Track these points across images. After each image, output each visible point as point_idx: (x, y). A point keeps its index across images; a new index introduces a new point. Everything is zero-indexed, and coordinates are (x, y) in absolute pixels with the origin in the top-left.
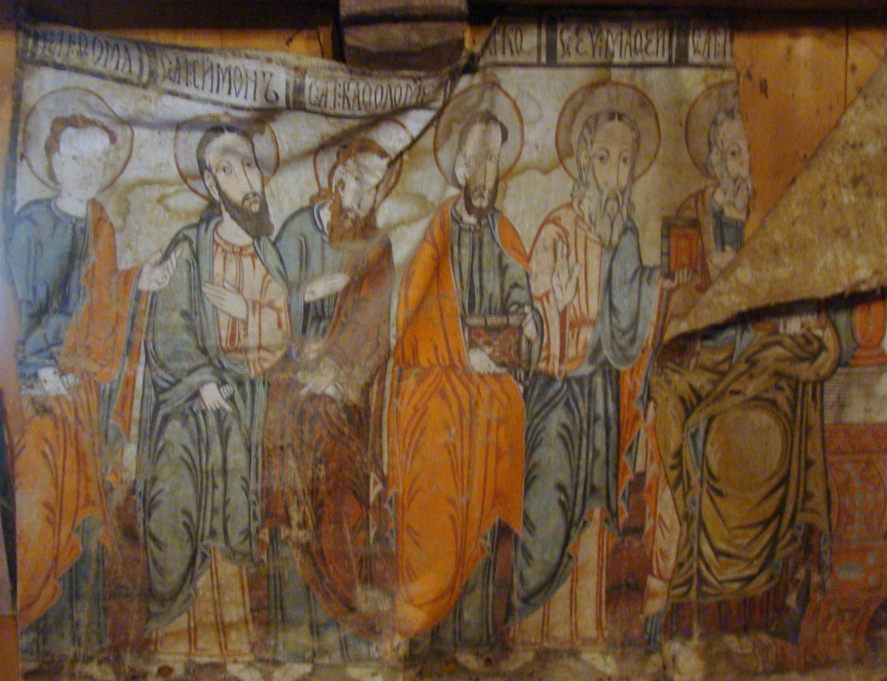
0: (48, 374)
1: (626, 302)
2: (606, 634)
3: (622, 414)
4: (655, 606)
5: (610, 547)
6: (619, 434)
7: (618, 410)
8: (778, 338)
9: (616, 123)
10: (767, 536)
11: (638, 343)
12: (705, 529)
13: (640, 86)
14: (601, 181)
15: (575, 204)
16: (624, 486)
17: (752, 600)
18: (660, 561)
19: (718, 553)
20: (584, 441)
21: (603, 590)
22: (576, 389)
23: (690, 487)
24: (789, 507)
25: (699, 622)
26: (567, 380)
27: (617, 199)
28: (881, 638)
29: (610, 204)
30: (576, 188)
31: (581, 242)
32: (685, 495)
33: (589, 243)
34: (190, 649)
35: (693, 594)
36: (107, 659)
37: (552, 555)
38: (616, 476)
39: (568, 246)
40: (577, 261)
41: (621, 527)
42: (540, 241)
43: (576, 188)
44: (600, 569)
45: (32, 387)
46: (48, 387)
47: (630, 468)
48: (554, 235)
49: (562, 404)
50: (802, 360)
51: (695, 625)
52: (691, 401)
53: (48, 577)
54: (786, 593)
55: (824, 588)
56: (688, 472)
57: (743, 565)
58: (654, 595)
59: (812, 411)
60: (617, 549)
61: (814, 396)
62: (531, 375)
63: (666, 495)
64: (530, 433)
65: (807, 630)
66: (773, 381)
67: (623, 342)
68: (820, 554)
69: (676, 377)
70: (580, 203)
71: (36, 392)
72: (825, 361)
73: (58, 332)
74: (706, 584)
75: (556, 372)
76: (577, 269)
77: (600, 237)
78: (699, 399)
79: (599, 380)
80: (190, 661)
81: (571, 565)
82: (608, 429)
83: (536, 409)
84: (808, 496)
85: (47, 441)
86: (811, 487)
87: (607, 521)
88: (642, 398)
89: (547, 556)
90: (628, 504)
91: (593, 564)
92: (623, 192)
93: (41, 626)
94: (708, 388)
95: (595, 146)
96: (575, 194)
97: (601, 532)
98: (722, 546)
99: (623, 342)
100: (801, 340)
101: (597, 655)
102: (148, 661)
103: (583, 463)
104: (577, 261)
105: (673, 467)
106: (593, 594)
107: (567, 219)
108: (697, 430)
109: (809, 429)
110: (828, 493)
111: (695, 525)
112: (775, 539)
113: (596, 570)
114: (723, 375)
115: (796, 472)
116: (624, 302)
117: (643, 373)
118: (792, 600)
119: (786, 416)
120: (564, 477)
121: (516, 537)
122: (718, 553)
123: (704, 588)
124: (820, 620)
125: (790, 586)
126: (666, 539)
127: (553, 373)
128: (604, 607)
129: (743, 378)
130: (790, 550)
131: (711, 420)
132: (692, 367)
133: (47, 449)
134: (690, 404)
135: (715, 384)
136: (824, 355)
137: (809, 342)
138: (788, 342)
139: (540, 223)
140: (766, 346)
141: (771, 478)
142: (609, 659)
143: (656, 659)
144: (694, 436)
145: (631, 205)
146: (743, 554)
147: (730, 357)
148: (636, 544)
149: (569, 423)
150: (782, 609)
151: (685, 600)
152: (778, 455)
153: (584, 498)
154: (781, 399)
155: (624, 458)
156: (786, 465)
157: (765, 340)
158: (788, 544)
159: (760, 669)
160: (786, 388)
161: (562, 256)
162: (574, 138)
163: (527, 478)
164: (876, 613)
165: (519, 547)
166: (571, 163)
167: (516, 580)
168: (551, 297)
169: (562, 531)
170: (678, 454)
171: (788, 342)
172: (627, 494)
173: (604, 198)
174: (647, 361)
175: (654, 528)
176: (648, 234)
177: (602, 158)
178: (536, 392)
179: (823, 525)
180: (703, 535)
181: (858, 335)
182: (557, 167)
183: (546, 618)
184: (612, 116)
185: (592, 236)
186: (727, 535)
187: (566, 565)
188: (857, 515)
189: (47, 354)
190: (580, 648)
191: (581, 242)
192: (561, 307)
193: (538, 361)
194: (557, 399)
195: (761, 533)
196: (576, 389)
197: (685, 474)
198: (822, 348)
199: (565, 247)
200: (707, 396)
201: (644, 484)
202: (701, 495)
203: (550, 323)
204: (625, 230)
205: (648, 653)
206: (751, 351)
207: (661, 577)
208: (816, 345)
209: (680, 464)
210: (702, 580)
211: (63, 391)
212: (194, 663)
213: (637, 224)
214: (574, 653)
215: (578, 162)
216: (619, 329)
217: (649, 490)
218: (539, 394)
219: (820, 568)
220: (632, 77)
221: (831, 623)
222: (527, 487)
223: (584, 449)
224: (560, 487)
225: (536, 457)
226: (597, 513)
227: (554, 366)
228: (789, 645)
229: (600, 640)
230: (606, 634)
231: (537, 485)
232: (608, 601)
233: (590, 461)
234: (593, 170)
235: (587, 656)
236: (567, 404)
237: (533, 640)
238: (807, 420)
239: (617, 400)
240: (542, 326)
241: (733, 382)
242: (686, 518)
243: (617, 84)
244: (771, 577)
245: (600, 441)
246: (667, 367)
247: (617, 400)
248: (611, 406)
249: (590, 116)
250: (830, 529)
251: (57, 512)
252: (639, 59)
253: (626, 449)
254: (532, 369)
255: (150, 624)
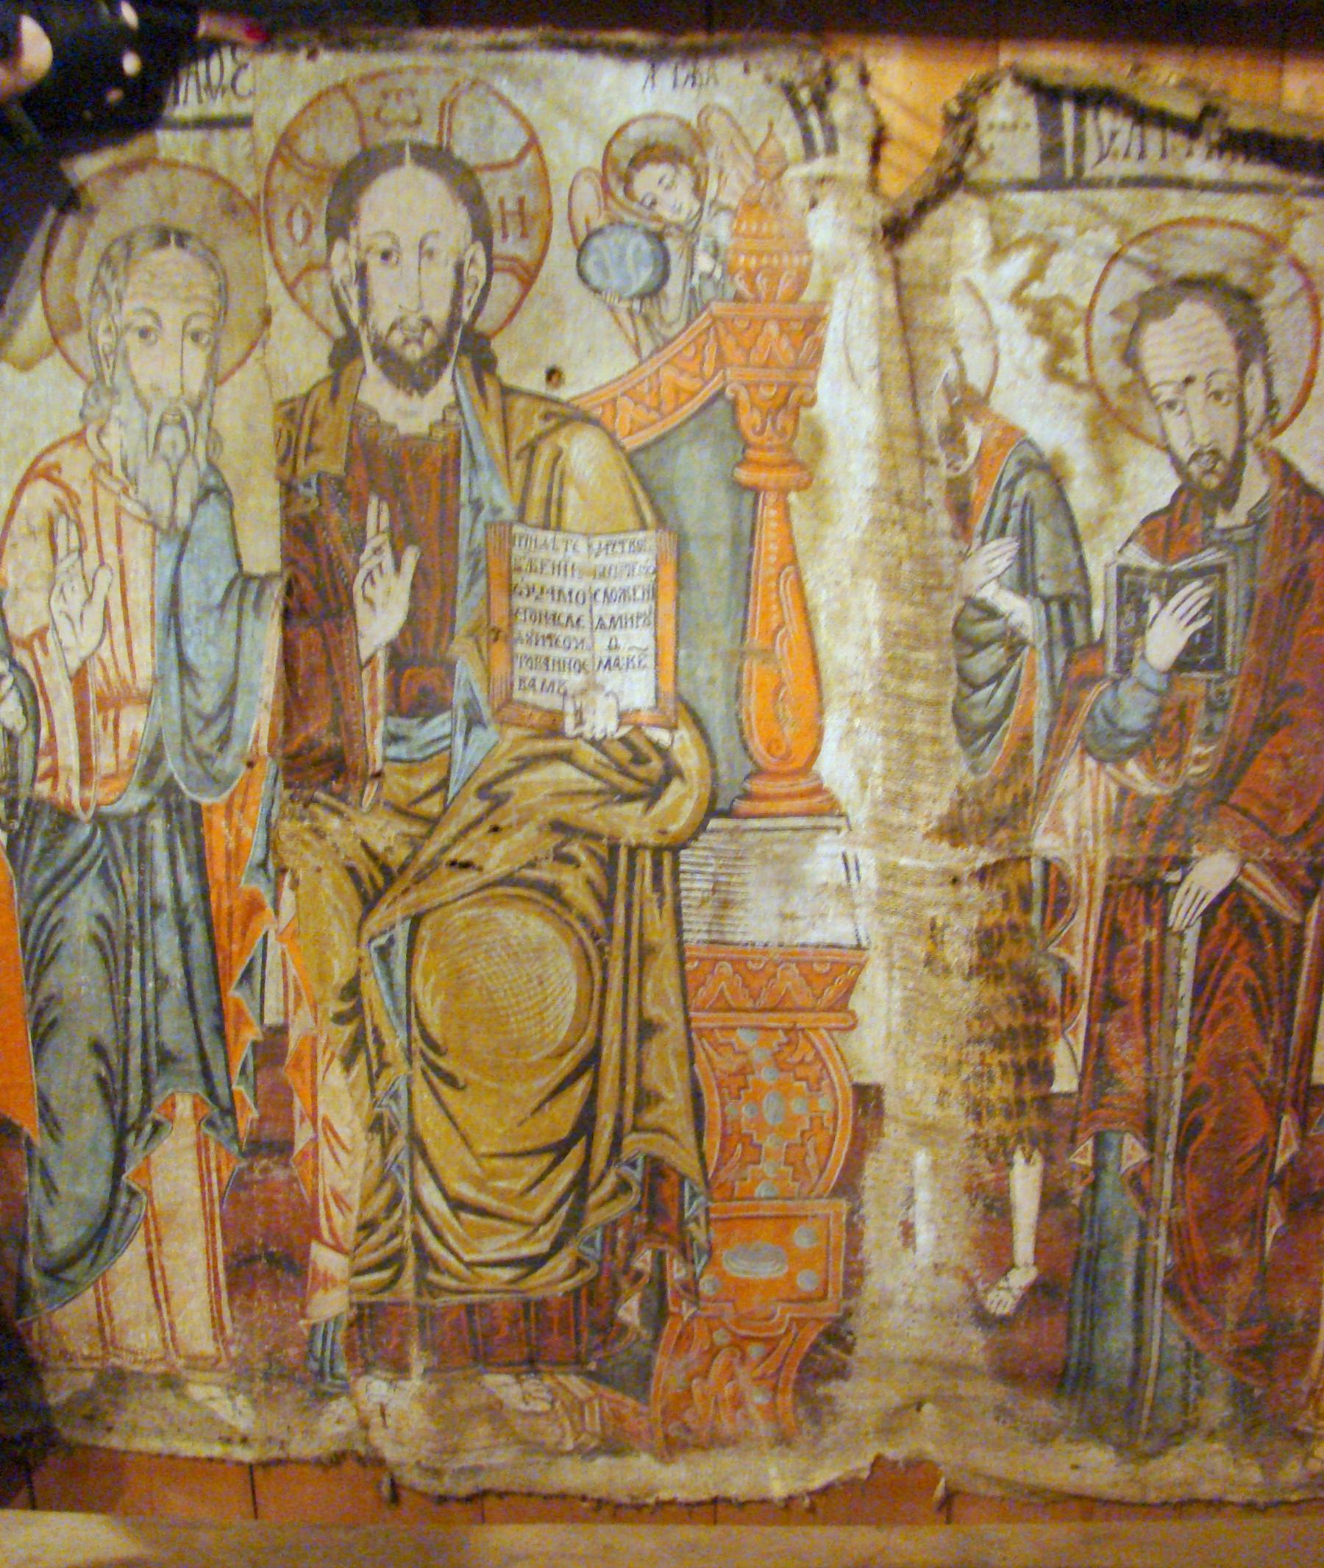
1: (213, 656)
2: (234, 1350)
3: (213, 897)
4: (330, 1305)
5: (226, 1174)
6: (212, 944)
7: (205, 894)
8: (562, 745)
9: (172, 251)
10: (565, 1176)
11: (235, 747)
12: (424, 1154)
13: (223, 171)
14: (144, 383)
15: (91, 436)
16: (243, 1053)
17: (542, 1304)
18: (334, 1209)
19: (458, 1205)
20: (136, 954)
21: (221, 1267)
22: (118, 838)
23: (383, 1065)
24: (606, 1121)
25: (423, 1347)
26: (100, 820)
27: (183, 424)
28: (829, 1399)
29: (167, 435)
30: (91, 399)
31: (108, 519)
32: (373, 1078)
33: (127, 525)
35: (407, 1285)
37: (93, 1187)
38: (220, 1030)
39: (80, 527)
40: (102, 563)
41: (243, 1135)
42: (19, 517)
43: (91, 399)
44: (210, 1219)
47: (252, 1016)
48: (49, 504)
49: (94, 871)
50: (631, 798)
51: (414, 1351)
52: (372, 878)
54: (616, 1297)
55: (697, 1293)
56: (375, 1030)
57: (518, 1233)
58: (327, 1281)
59: (652, 911)
60: (240, 1182)
61: (657, 878)
62: (21, 808)
63: (334, 1079)
64: (32, 931)
65: (669, 1371)
66: (551, 841)
67: (206, 741)
68: (682, 1223)
69: (334, 823)
70: (101, 432)
72: (680, 804)
74: (438, 1269)
75: (76, 803)
76: (104, 578)
77: (147, 509)
78: (385, 869)
79: (157, 824)
81: (138, 1210)
82: (184, 931)
83: (39, 884)
84: (646, 1099)
86: (653, 1076)
87: (211, 1123)
88: (263, 865)
89: (83, 1190)
90: (255, 1087)
91: (191, 1209)
92: (196, 409)
94: (402, 853)
95: (129, 306)
96: (87, 412)
97: (201, 1146)
98: (467, 1191)
99: (206, 741)
100: (624, 755)
101: (215, 1391)
103: (135, 1000)
104: (102, 563)
105: (340, 1019)
106: (201, 1270)
107: (75, 466)
108: (391, 941)
109: (646, 952)
110: (696, 1095)
111: (401, 1143)
112: (581, 1185)
113: (201, 1224)
114: (433, 823)
115: (616, 1047)
116: (207, 654)
117: (257, 812)
118: (630, 1311)
119: (584, 919)
120: (103, 1027)
121: (29, 1143)
122: (458, 1205)
123: (432, 1276)
124: (694, 1354)
125: (625, 1284)
126: (342, 1169)
127: (69, 803)
128: (224, 1295)
129: (475, 835)
130: (618, 1209)
131: (416, 922)
132: (367, 802)
134: (374, 883)
135: (416, 845)
136: (675, 787)
137: (639, 759)
138: (589, 755)
139: (19, 474)
140: (527, 763)
141: (561, 1054)
142: (241, 1400)
143: (339, 1407)
144: (384, 952)
145: (215, 438)
146: (517, 1212)
147: (443, 784)
148: (279, 1174)
149: (107, 912)
150: (609, 1328)
151: (386, 1297)
152: (571, 1008)
153: (145, 1072)
154: (573, 884)
155: (234, 994)
156: (591, 1031)
157: (525, 749)
158: (614, 1196)
159: (569, 1445)
160: (583, 858)
161: (69, 552)
162: (83, 289)
163: (35, 1027)
164: (815, 1347)
165: (37, 1166)
166: (76, 344)
167: (32, 1231)
168: (50, 636)
169: (107, 1140)
170: (352, 989)
171: (589, 755)
172: (250, 1069)
173: (154, 421)
174: (262, 789)
175: (315, 1140)
176: (252, 502)
177: (144, 333)
178: (36, 848)
179: (682, 1158)
180: (420, 1164)
181: (757, 745)
182: (47, 354)
183: (104, 1313)
184: (163, 237)
185: (129, 505)
186: (477, 1171)
187: (127, 1211)
188: (768, 1143)
190: (184, 1373)
191: (108, 519)
192: (74, 663)
193: (34, 779)
194: (83, 863)
195: (551, 1168)
196: (118, 838)
197: (370, 1039)
198: (671, 772)
199: (73, 529)
200: (403, 868)
201: (284, 1056)
202: (410, 1081)
203: (51, 697)
204: (206, 493)
205: (322, 1398)
206: (489, 774)
207: (338, 1248)
208: (656, 764)
209: (358, 1011)
210: (426, 1260)
213: (229, 477)
214: (172, 1382)
215: (92, 341)
216: (199, 714)
217: (297, 1065)
218: (44, 851)
219: (684, 1250)
220: (204, 150)
221: (719, 1362)
222: (39, 1045)
223: (135, 972)
224: (98, 1049)
225: (50, 983)
226: (184, 1106)
227: (69, 791)
228: (630, 1401)
229: (224, 1364)
230: (234, 1350)
231: (58, 1039)
232: (233, 1286)
233: (150, 997)
234: (126, 357)
235: (197, 1391)
236: (104, 871)
237: (86, 1352)
238: (641, 935)
239: (200, 867)
240: (35, 699)
241: (455, 840)
242: (376, 1125)
243: (170, 165)
244: (580, 1264)
245: (168, 957)
246: (316, 801)
247: (200, 867)
248: (188, 883)
249: (115, 241)
250: (704, 1166)
252: (217, 108)
253: (238, 974)
254: (24, 793)
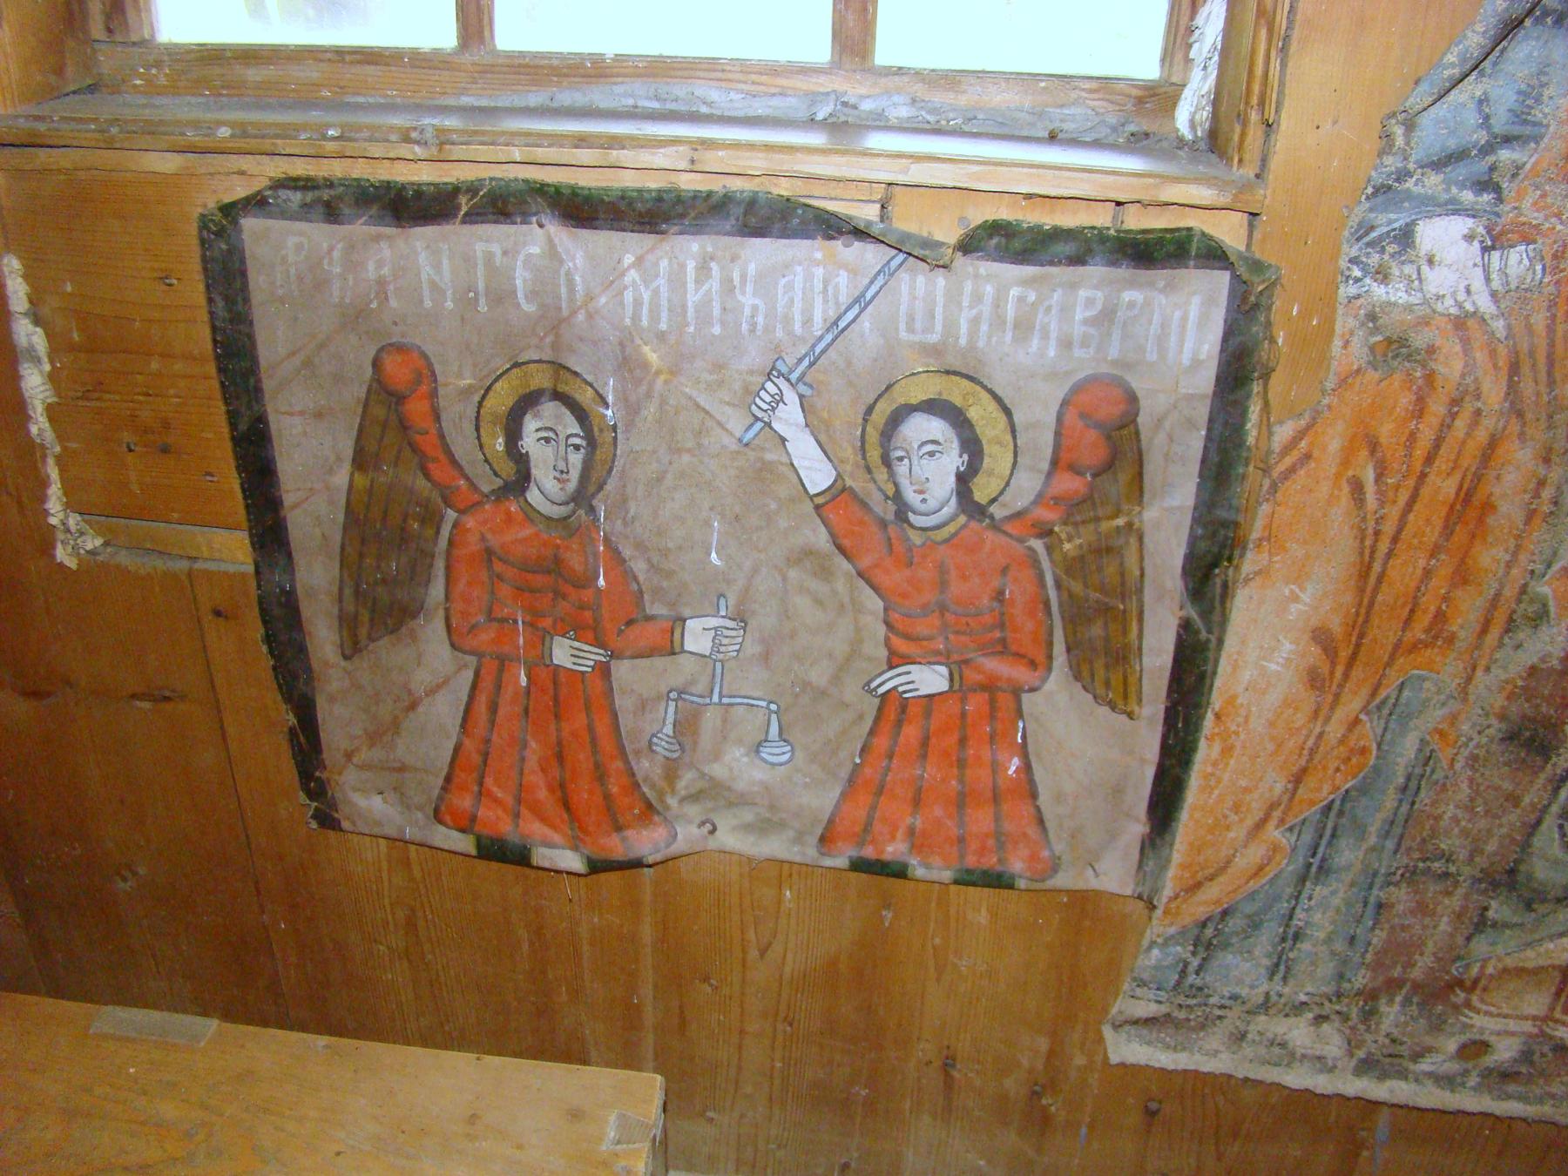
0: (1446, 239)
34: (1552, 1009)
36: (1345, 1017)
45: (1382, 275)
46: (1438, 281)
53: (1260, 825)
71: (1394, 293)
73: (1531, 95)
80: (1542, 1033)
85: (1374, 446)
93: (1209, 932)
102: (1437, 1027)
133: (1369, 476)
189: (1480, 167)
211: (1485, 304)
212: (1551, 1038)
251: (1344, 654)
255: (1473, 944)
